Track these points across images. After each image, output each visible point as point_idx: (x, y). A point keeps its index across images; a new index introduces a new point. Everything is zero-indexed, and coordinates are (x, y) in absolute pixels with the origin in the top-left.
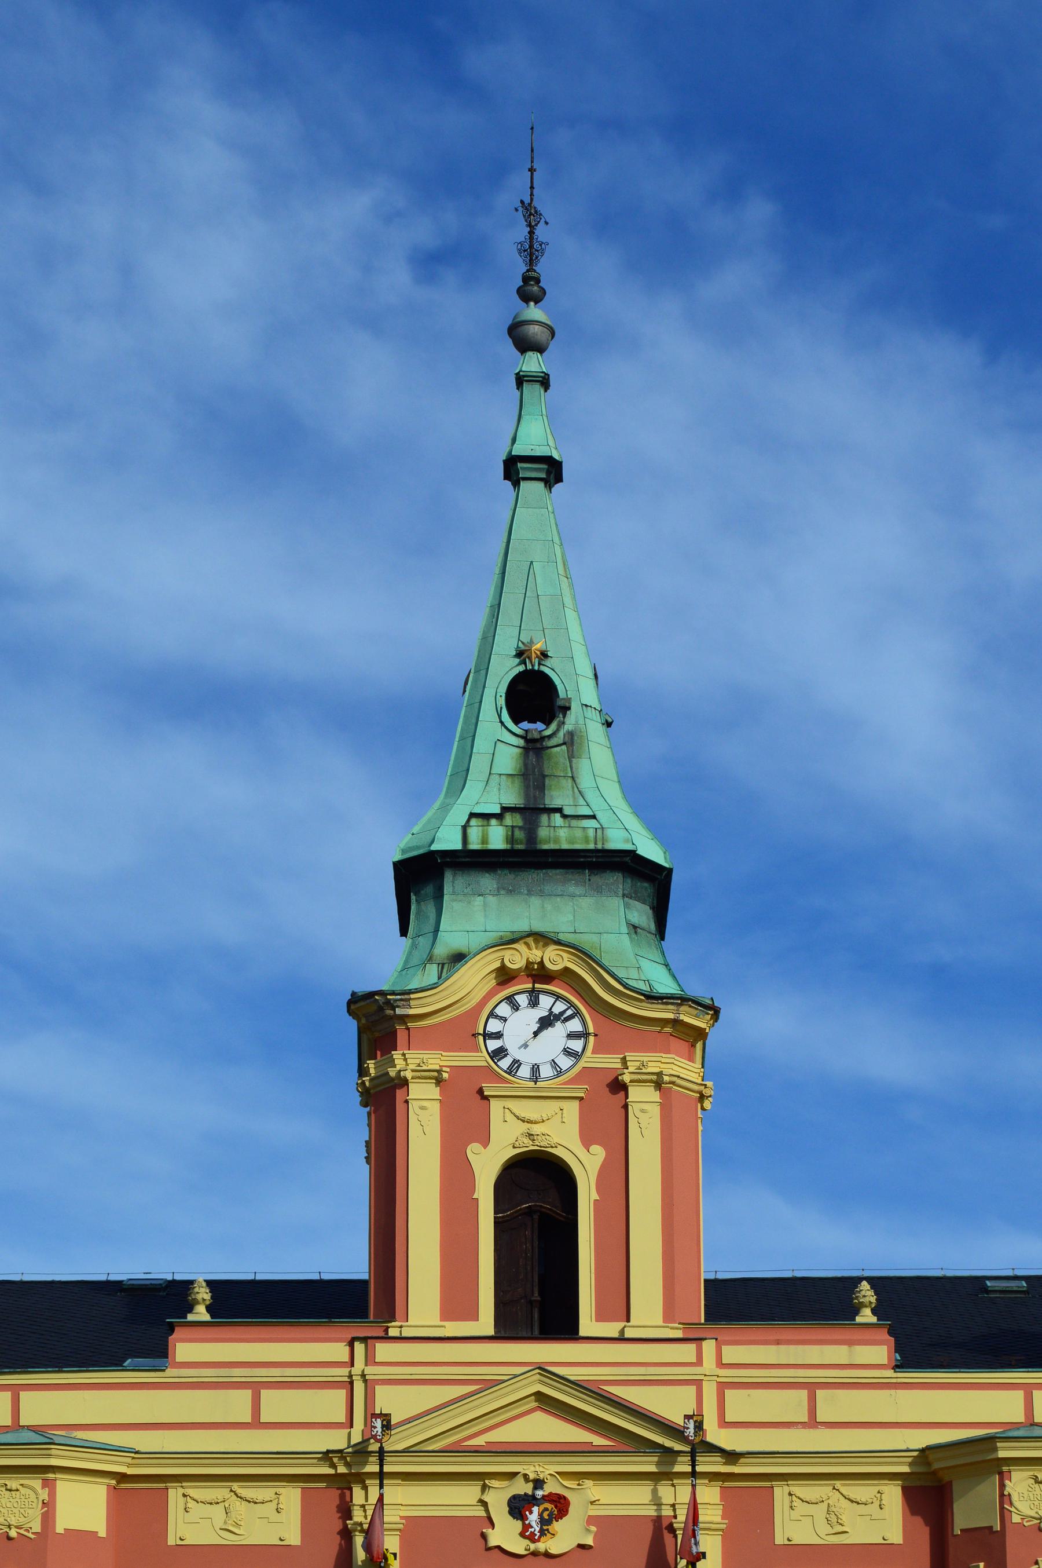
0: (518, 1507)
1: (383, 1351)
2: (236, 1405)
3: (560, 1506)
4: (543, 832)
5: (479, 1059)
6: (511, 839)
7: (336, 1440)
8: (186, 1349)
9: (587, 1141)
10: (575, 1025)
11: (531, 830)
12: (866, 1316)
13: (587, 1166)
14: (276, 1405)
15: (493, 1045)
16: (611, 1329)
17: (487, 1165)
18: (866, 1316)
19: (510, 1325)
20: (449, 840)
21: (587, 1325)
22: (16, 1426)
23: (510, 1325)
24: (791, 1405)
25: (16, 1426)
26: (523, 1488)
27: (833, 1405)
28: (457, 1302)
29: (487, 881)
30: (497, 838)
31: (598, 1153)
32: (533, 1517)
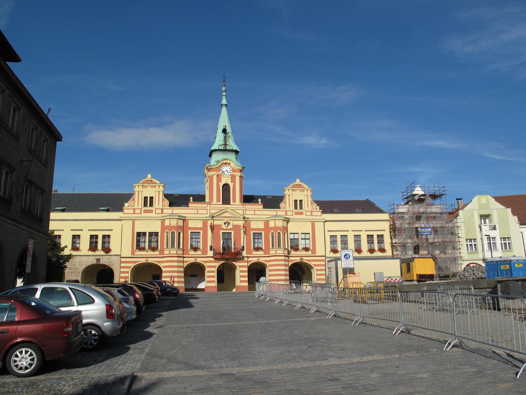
0: (225, 223)
1: (211, 206)
2: (196, 211)
3: (229, 223)
5: (220, 173)
8: (190, 205)
9: (232, 182)
12: (260, 203)
13: (231, 185)
14: (200, 212)
17: (221, 185)
18: (260, 203)
19: (223, 203)
21: (231, 203)
22: (173, 214)
23: (223, 203)
24: (253, 212)
25: (173, 214)
27: (257, 213)
28: (218, 200)
31: (233, 184)
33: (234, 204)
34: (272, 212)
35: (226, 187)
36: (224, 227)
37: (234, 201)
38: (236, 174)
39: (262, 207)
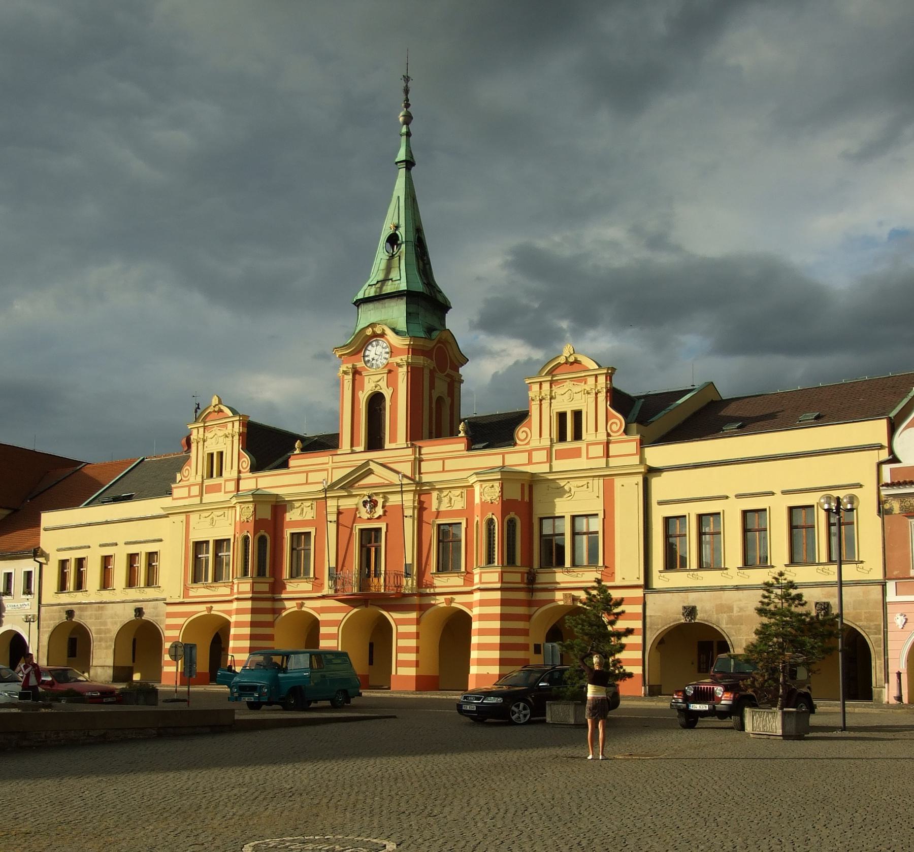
0: (365, 503)
1: (336, 458)
4: (384, 288)
6: (376, 292)
7: (321, 487)
10: (388, 350)
11: (381, 288)
12: (462, 434)
13: (387, 393)
15: (367, 359)
16: (393, 446)
17: (363, 398)
18: (462, 434)
20: (360, 296)
21: (387, 445)
24: (438, 466)
26: (366, 498)
27: (449, 465)
29: (371, 306)
30: (372, 292)
31: (391, 391)
32: (368, 507)
33: (393, 446)
34: (491, 458)
35: (376, 401)
36: (364, 513)
37: (393, 439)
38: (397, 359)
39: (462, 446)
